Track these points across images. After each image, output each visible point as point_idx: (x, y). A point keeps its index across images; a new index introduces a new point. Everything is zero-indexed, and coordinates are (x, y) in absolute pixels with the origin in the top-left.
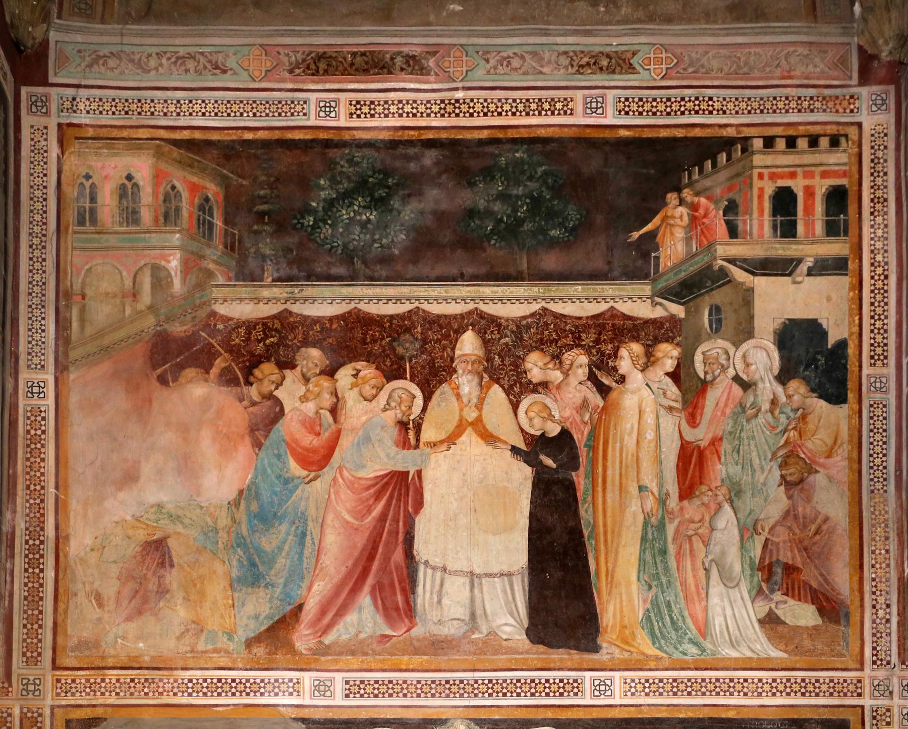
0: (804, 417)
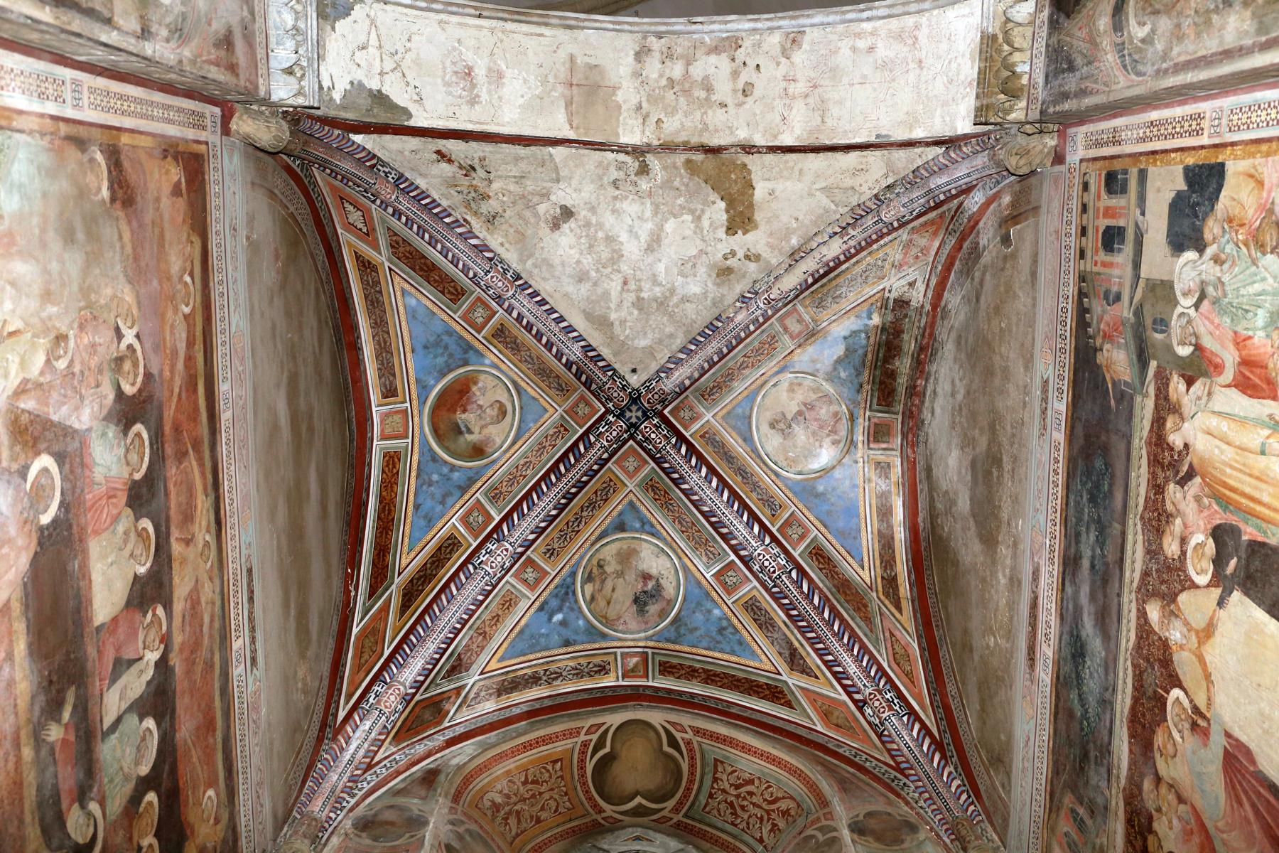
0: (1230, 220)
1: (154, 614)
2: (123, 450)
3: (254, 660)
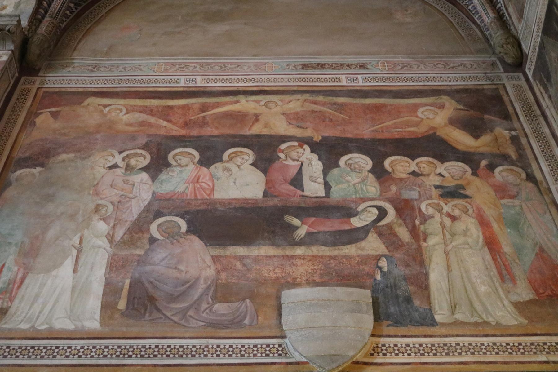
1: (283, 151)
2: (178, 169)
3: (363, 66)
